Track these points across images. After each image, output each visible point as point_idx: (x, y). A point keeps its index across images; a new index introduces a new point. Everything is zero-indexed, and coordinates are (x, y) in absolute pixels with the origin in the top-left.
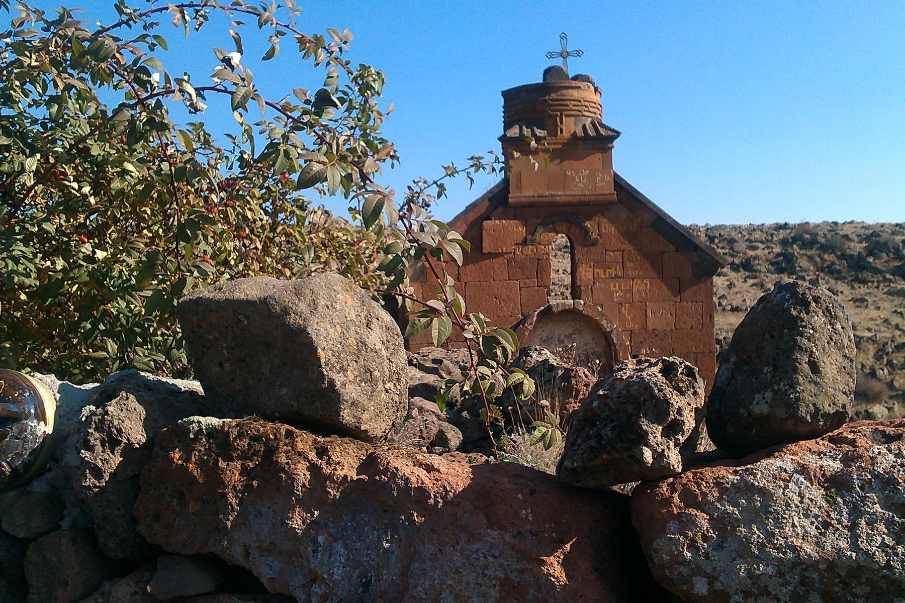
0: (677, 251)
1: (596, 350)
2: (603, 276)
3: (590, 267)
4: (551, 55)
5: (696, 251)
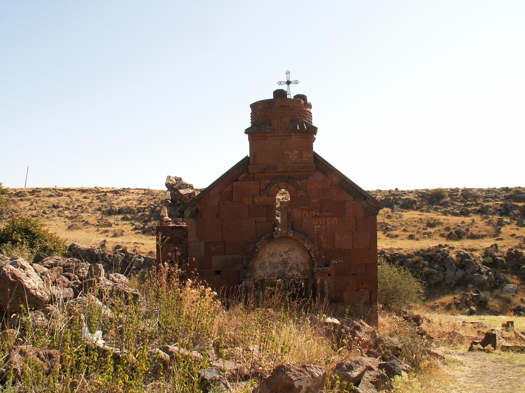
2: (308, 216)
3: (300, 210)
4: (280, 83)
5: (365, 200)
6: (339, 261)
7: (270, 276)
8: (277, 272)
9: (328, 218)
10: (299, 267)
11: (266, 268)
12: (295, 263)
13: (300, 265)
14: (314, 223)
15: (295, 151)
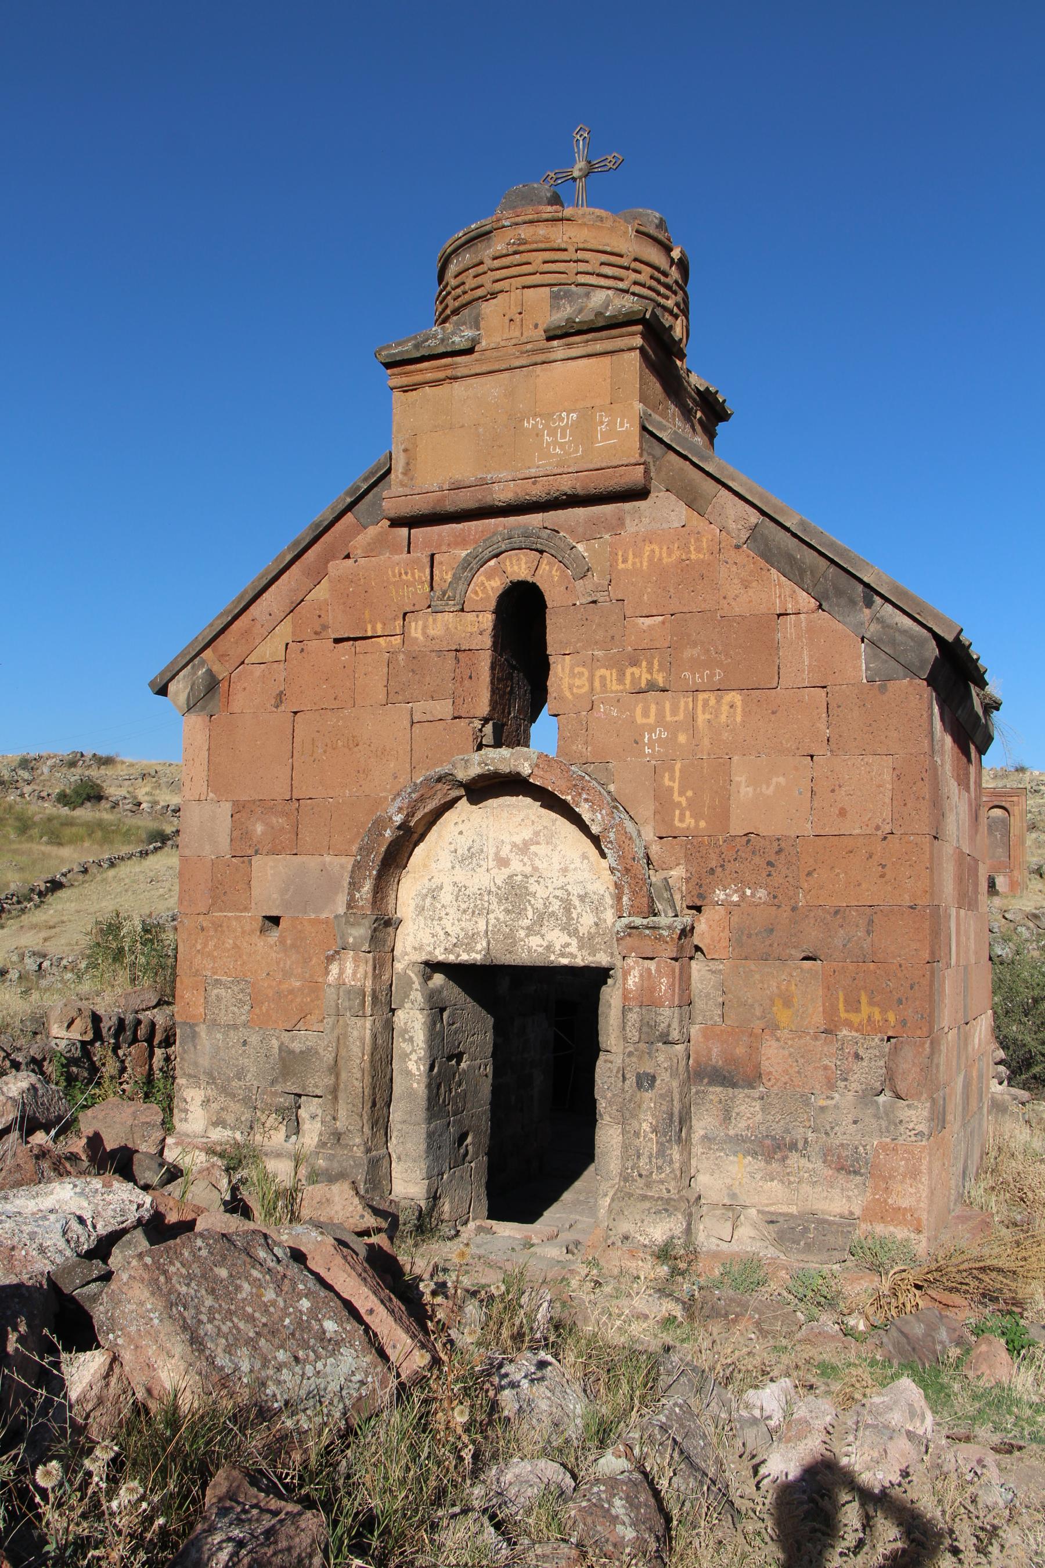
0: (820, 606)
1: (590, 888)
2: (615, 687)
6: (748, 892)
7: (455, 945)
8: (482, 934)
9: (701, 696)
10: (574, 915)
11: (443, 914)
12: (557, 897)
13: (576, 902)
14: (640, 720)
15: (564, 414)
